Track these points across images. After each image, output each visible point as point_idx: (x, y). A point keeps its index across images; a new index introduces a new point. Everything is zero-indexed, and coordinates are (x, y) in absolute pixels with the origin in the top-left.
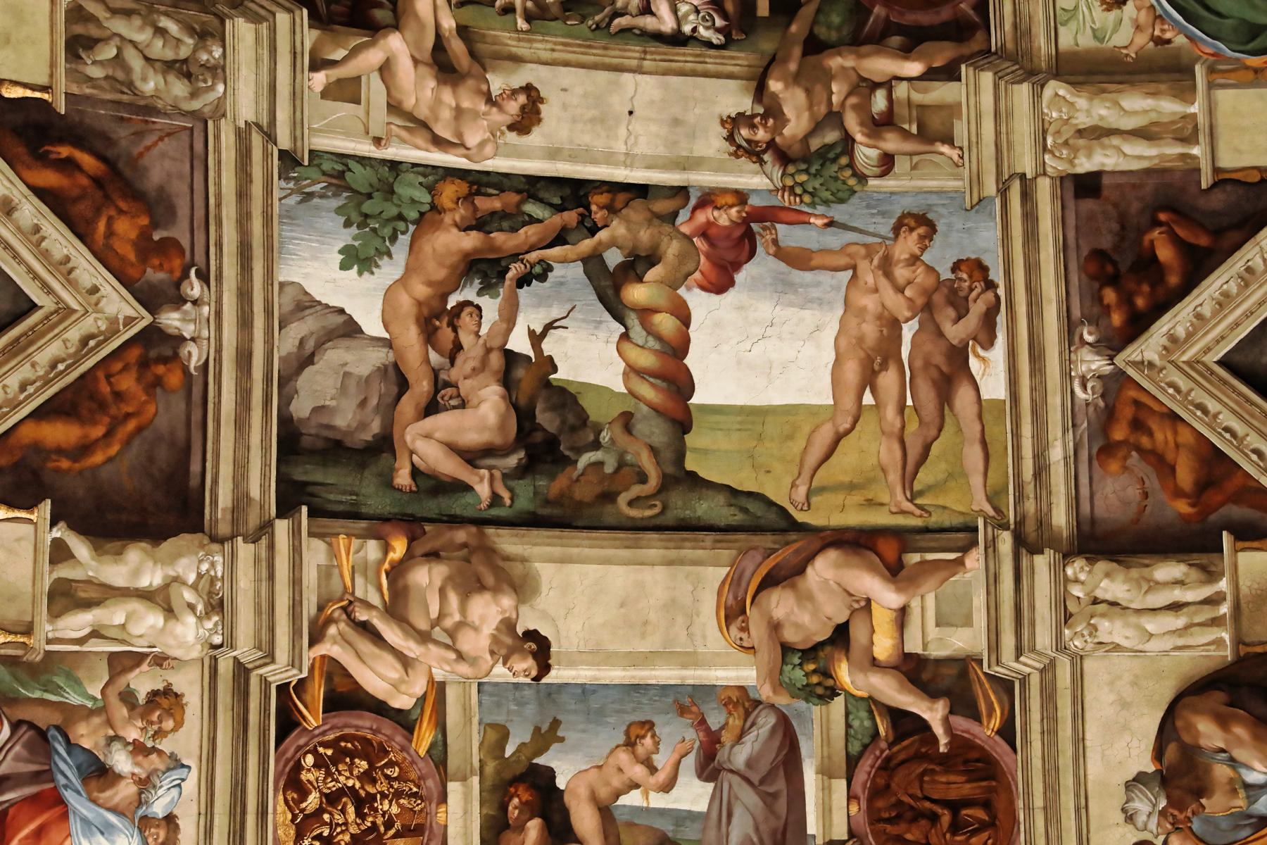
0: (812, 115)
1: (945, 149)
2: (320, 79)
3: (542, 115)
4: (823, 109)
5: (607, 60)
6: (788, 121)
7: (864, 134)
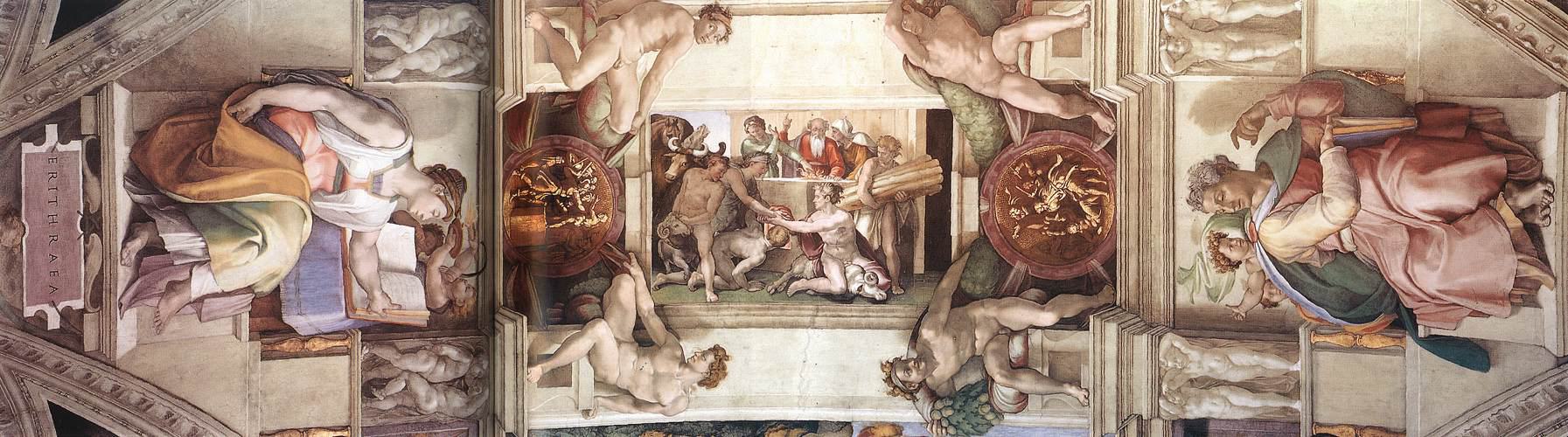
0: (958, 359)
1: (1072, 390)
2: (537, 372)
3: (727, 371)
4: (968, 354)
5: (784, 319)
6: (938, 364)
7: (1002, 376)
